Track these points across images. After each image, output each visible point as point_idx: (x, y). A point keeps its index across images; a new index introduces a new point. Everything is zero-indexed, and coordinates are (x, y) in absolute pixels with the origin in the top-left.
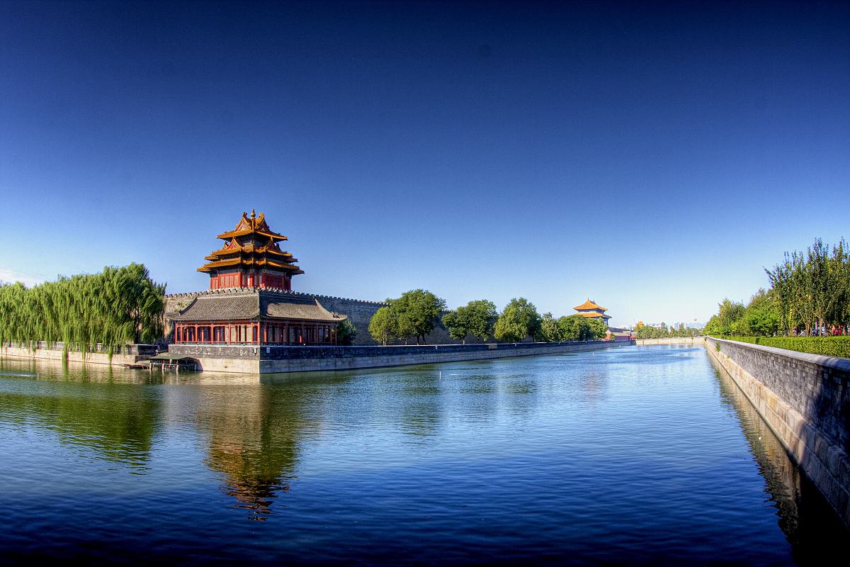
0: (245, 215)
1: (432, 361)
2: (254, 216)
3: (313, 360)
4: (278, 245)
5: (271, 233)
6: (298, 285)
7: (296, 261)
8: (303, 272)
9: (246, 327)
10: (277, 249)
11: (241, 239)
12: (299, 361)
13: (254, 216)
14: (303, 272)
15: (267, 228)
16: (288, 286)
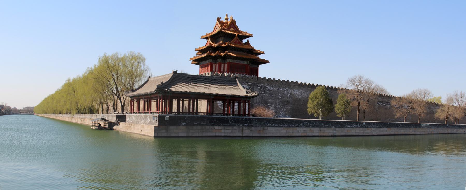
0: (218, 20)
1: (357, 134)
2: (227, 19)
3: (217, 128)
4: (248, 41)
5: (239, 32)
6: (264, 72)
7: (263, 53)
8: (267, 62)
9: (183, 101)
10: (248, 43)
11: (214, 37)
12: (199, 127)
13: (227, 19)
14: (267, 62)
15: (237, 30)
16: (256, 72)
